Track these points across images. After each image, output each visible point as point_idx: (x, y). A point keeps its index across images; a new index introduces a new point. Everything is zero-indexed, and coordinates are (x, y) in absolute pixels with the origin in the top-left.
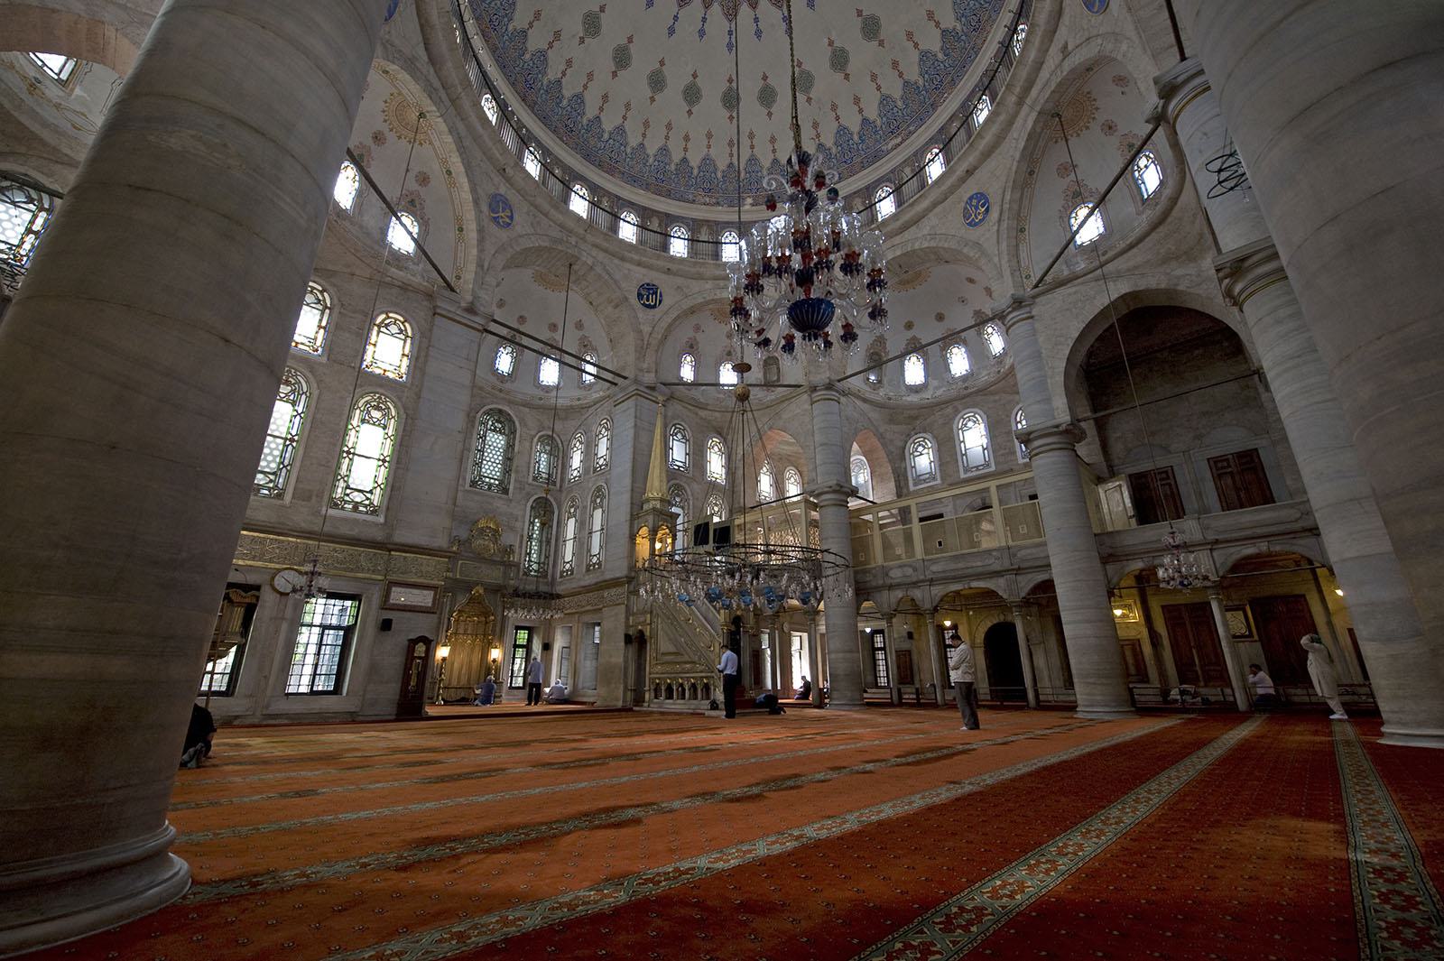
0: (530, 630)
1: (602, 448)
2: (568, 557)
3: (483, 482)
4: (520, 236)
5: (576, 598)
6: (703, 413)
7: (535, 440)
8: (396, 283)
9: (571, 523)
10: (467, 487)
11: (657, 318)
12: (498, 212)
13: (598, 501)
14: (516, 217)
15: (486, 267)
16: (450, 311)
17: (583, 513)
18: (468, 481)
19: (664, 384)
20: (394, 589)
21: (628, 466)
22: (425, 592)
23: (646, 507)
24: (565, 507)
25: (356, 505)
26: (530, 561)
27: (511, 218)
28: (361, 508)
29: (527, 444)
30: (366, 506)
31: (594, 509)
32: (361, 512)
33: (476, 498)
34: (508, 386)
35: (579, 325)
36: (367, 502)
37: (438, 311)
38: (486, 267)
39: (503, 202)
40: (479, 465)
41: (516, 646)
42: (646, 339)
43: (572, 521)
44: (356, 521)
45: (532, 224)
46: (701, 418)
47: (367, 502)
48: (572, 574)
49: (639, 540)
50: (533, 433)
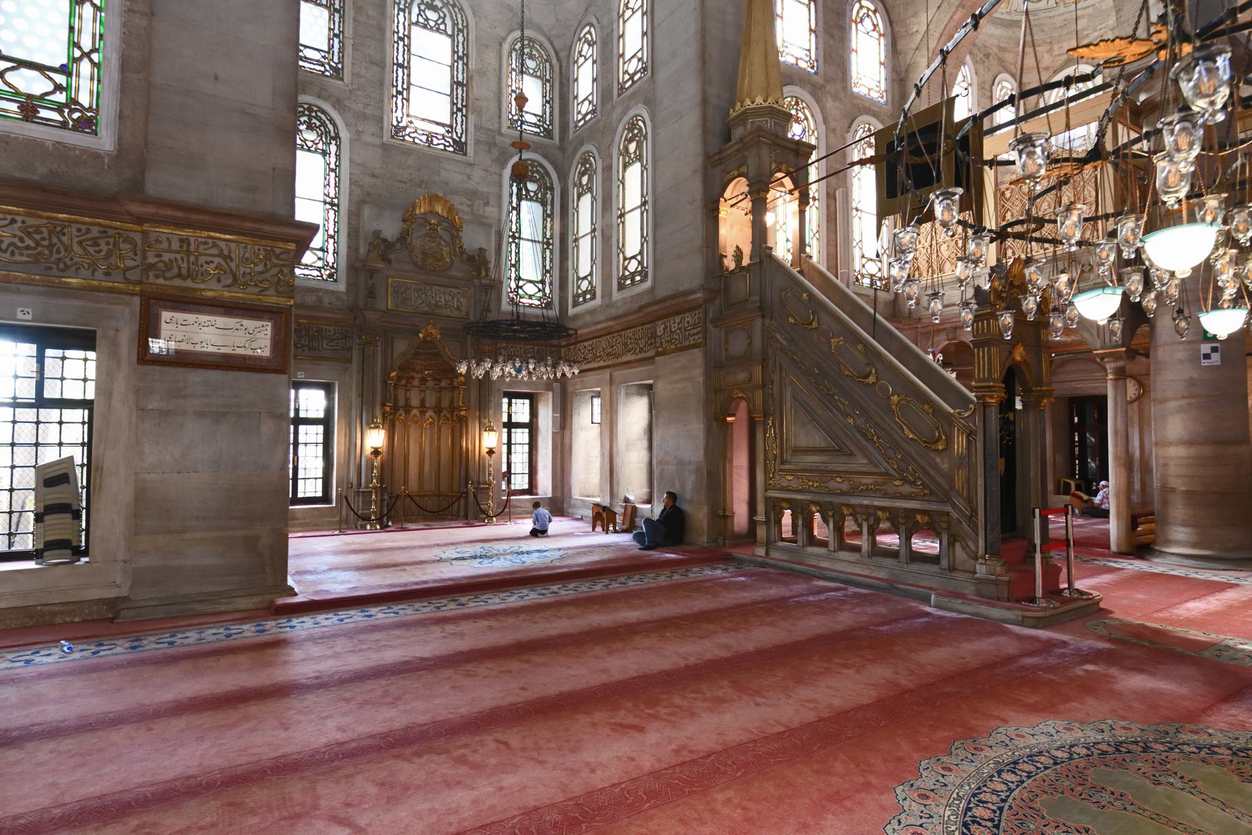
0: (533, 399)
1: (633, 37)
2: (584, 268)
5: (603, 343)
7: (506, 47)
9: (586, 200)
13: (632, 147)
17: (607, 180)
20: (166, 315)
21: (690, 51)
22: (249, 324)
23: (738, 133)
24: (573, 175)
25: (29, 106)
26: (518, 278)
28: (44, 113)
29: (491, 57)
31: (625, 166)
32: (46, 122)
36: (60, 97)
41: (510, 425)
43: (586, 200)
44: (34, 145)
47: (60, 97)
48: (593, 297)
49: (725, 212)
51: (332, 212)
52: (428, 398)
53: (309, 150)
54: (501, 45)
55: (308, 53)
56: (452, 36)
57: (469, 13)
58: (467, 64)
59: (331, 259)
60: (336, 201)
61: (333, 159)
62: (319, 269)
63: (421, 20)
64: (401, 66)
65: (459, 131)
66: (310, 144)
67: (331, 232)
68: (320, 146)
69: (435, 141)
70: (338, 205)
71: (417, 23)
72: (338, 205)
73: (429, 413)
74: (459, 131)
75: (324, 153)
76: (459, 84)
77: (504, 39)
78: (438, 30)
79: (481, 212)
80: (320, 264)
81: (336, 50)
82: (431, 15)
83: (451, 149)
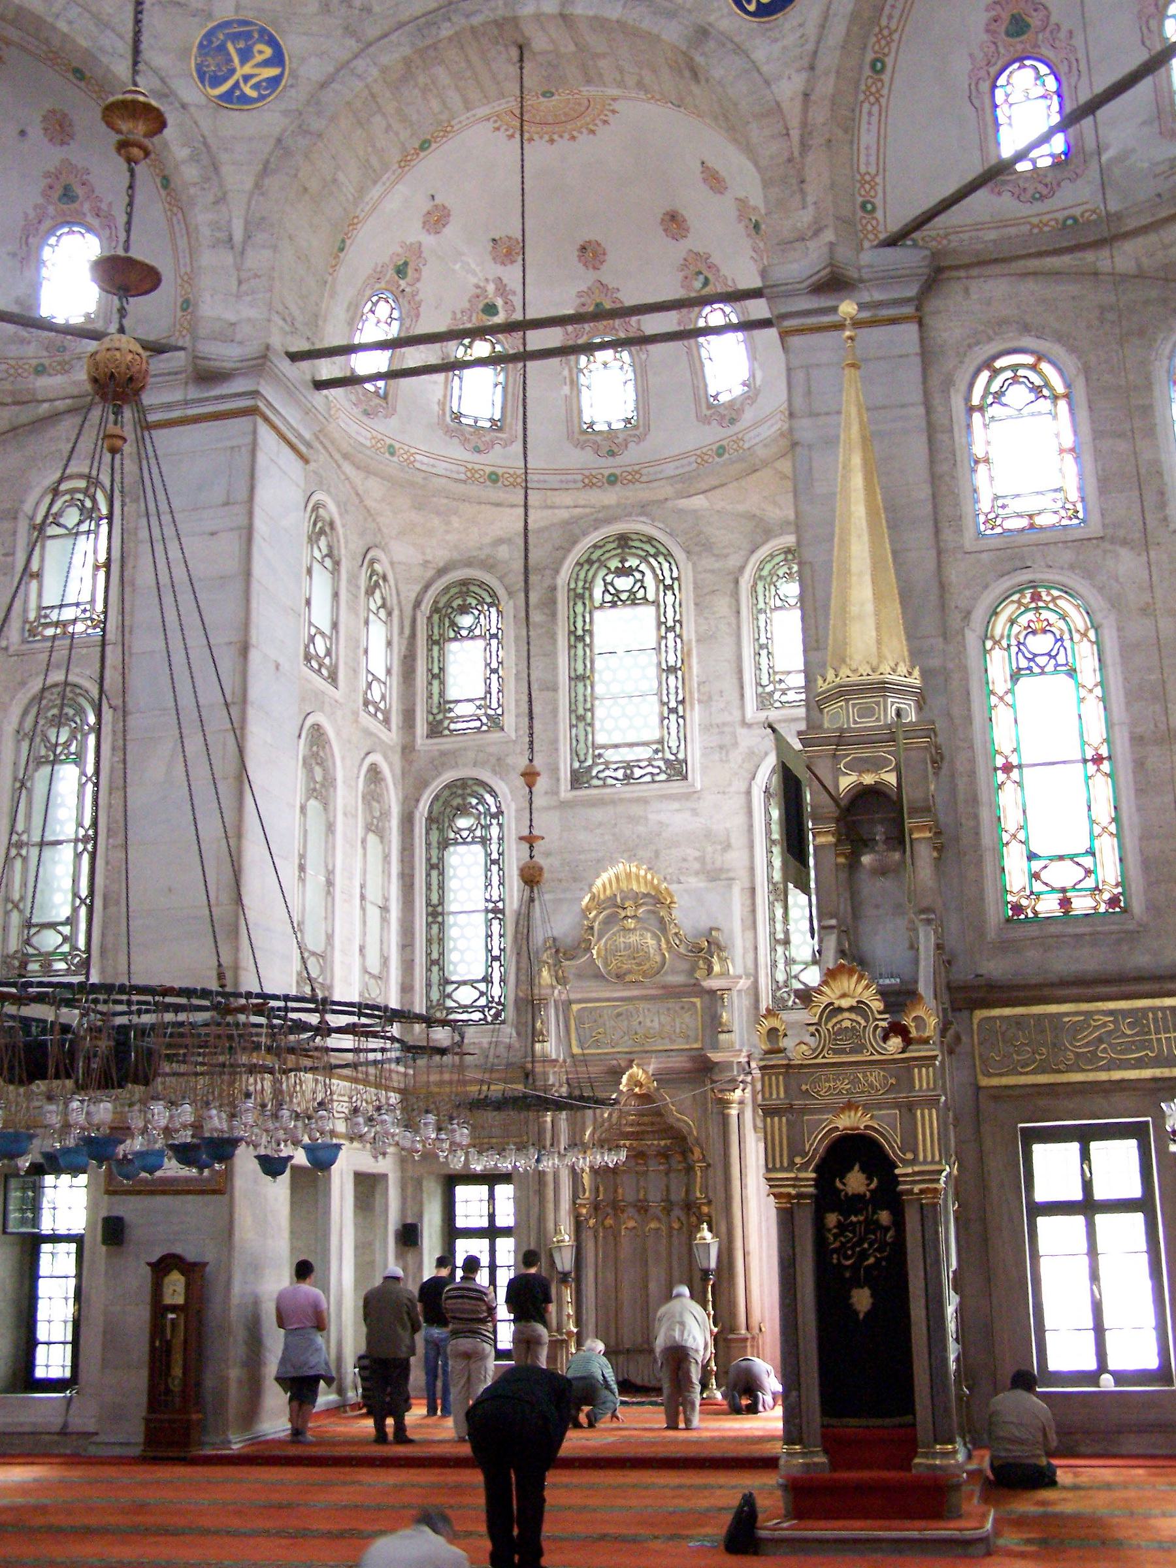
3: (607, 763)
4: (323, 85)
6: (1125, 257)
8: (60, 405)
10: (565, 791)
11: (811, 30)
12: (233, 71)
14: (291, 44)
15: (238, 236)
16: (169, 406)
18: (565, 775)
19: (893, 242)
27: (277, 59)
30: (64, 957)
33: (598, 814)
34: (632, 455)
35: (714, 180)
37: (152, 418)
38: (238, 236)
39: (235, 37)
40: (582, 717)
42: (794, 123)
45: (346, 28)
46: (1120, 279)
50: (733, 561)
51: (496, 923)
52: (673, 1188)
53: (465, 843)
54: (737, 582)
55: (461, 710)
56: (656, 603)
57: (679, 555)
58: (680, 636)
59: (496, 991)
60: (500, 905)
61: (494, 847)
62: (481, 1009)
63: (608, 598)
64: (582, 678)
65: (674, 744)
66: (465, 834)
67: (496, 952)
68: (478, 833)
69: (638, 772)
70: (502, 911)
71: (601, 607)
72: (502, 911)
73: (677, 1212)
74: (674, 744)
75: (484, 841)
76: (671, 670)
77: (742, 568)
78: (633, 601)
79: (718, 864)
80: (483, 1001)
81: (494, 690)
82: (623, 583)
83: (663, 777)
